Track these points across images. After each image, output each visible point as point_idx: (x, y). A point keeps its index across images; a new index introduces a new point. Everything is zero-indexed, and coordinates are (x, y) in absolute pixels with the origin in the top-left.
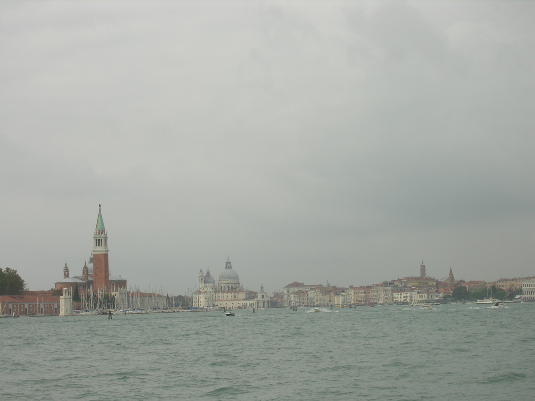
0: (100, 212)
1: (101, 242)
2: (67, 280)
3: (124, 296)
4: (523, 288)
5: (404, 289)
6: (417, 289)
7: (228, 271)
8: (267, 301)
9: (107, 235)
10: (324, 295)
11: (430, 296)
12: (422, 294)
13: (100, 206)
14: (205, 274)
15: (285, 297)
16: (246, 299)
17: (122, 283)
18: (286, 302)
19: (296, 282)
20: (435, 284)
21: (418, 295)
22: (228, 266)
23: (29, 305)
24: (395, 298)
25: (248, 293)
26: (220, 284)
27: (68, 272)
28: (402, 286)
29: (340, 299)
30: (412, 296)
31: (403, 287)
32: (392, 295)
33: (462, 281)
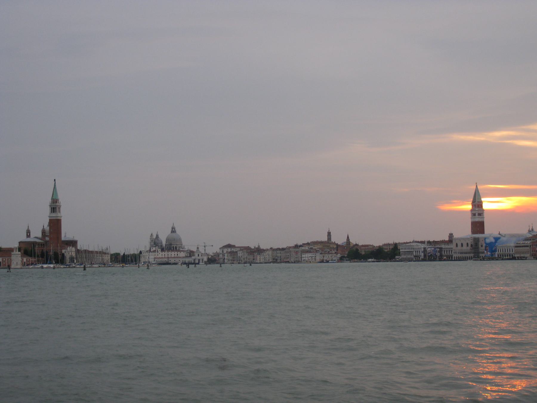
0: (55, 185)
1: (56, 209)
2: (29, 240)
3: (73, 253)
4: (401, 250)
6: (320, 250)
7: (174, 234)
8: (201, 259)
9: (60, 204)
10: (249, 254)
12: (323, 255)
13: (55, 180)
14: (154, 237)
15: (221, 256)
16: (186, 257)
17: (73, 243)
18: (221, 259)
20: (335, 246)
21: (321, 255)
22: (173, 231)
25: (188, 252)
27: (30, 233)
32: (301, 255)
33: (357, 245)
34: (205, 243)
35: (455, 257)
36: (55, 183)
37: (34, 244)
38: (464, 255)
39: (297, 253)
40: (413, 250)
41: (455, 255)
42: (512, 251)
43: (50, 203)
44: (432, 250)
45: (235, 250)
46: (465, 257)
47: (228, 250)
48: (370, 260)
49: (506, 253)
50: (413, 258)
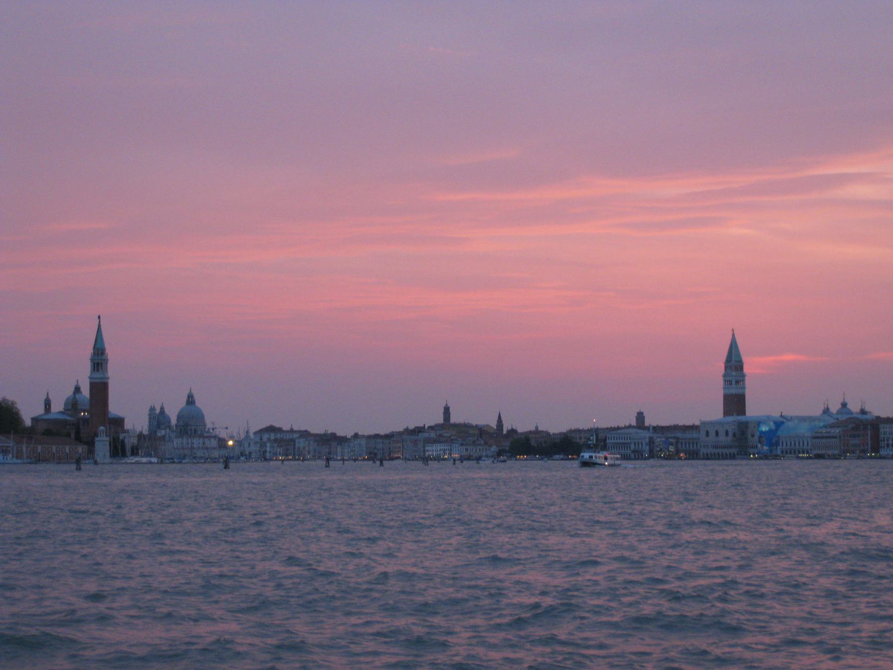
4: (608, 441)
10: (320, 444)
12: (467, 447)
20: (476, 432)
21: (462, 447)
22: (191, 400)
24: (427, 451)
28: (436, 435)
29: (346, 451)
32: (424, 447)
34: (213, 423)
37: (55, 421)
38: (720, 451)
39: (415, 442)
41: (703, 451)
44: (662, 441)
46: (722, 454)
47: (270, 435)
48: (557, 457)
50: (630, 455)
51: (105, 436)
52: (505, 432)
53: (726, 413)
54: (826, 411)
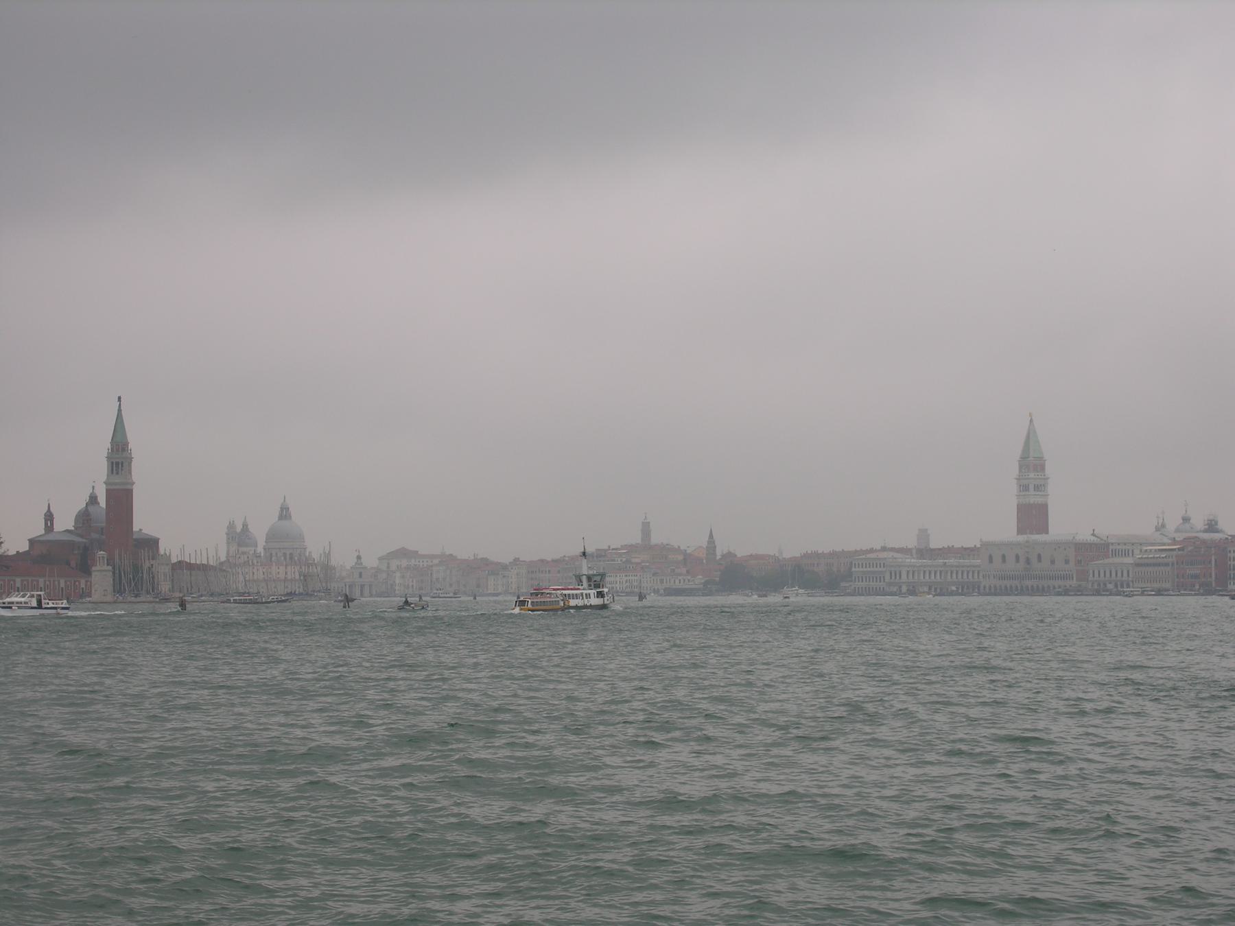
2: (50, 537)
4: (853, 569)
5: (626, 567)
9: (131, 453)
11: (677, 581)
14: (239, 529)
19: (403, 548)
20: (680, 558)
22: (285, 513)
23: (22, 581)
26: (269, 549)
27: (53, 521)
28: (621, 560)
30: (642, 580)
31: (624, 563)
33: (730, 555)
35: (985, 587)
36: (120, 405)
40: (882, 569)
42: (1128, 576)
43: (108, 453)
45: (419, 562)
46: (1011, 587)
49: (1124, 579)
51: (106, 565)
52: (718, 557)
53: (1020, 531)
54: (1160, 528)
